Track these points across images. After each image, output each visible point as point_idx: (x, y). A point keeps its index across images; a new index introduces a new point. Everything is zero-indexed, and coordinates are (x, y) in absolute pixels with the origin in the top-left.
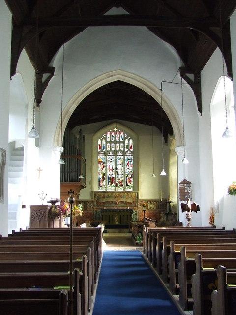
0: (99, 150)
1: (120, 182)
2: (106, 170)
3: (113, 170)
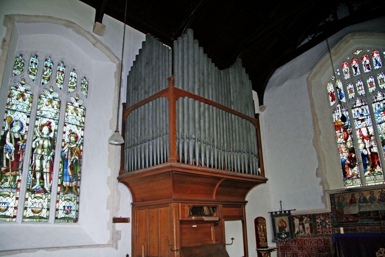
0: (332, 104)
3: (369, 137)
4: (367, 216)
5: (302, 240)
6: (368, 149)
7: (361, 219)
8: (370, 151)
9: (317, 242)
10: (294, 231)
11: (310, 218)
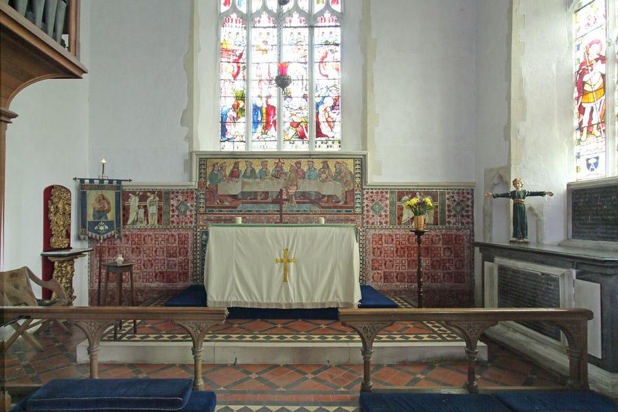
0: (224, 9)
1: (295, 125)
2: (246, 80)
4: (251, 199)
5: (140, 236)
6: (264, 99)
7: (243, 203)
8: (267, 102)
9: (168, 239)
10: (128, 219)
11: (160, 197)
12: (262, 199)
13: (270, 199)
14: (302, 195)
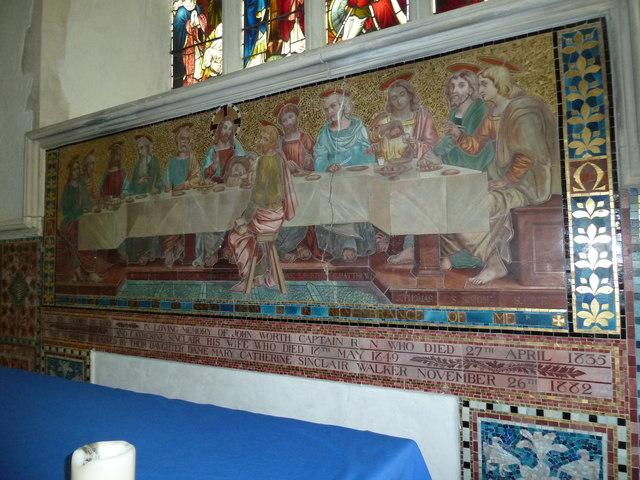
12: (177, 263)
13: (198, 263)
14: (305, 243)
